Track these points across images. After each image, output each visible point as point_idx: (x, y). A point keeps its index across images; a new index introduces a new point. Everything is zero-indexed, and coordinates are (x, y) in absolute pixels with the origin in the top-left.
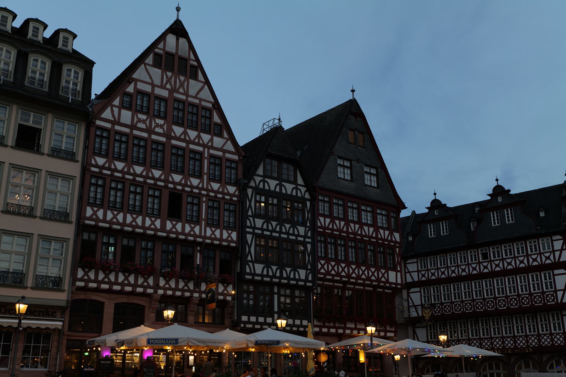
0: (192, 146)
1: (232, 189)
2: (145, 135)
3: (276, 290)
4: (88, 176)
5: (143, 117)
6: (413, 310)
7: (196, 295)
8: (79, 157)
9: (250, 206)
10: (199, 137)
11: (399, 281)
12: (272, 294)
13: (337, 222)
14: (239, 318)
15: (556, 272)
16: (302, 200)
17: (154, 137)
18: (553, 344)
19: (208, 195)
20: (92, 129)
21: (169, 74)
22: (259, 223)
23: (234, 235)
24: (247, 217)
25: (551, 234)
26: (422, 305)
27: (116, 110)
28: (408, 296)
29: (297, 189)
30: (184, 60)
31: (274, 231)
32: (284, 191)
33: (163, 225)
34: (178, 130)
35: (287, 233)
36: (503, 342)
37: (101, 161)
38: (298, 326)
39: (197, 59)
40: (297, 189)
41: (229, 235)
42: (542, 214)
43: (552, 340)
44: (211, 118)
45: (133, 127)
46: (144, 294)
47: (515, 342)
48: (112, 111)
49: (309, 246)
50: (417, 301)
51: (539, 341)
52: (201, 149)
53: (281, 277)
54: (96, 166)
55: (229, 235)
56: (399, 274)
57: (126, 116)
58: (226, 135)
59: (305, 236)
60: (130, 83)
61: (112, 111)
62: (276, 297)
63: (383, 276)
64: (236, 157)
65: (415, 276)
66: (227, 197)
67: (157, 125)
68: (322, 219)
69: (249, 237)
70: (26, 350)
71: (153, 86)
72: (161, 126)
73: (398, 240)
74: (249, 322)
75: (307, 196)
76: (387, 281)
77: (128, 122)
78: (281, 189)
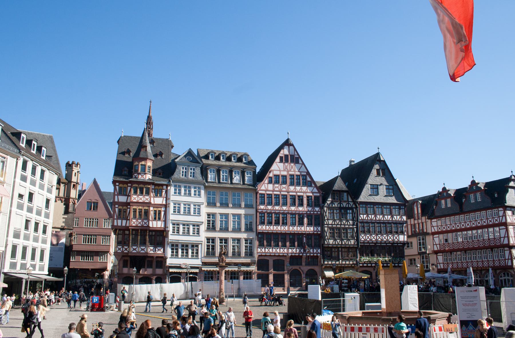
0: (298, 194)
1: (317, 209)
2: (278, 193)
3: (340, 249)
4: (258, 214)
5: (277, 185)
6: (435, 246)
7: (305, 254)
8: (255, 206)
9: (326, 215)
10: (301, 189)
11: (406, 240)
12: (338, 251)
13: (370, 216)
14: (324, 262)
15: (501, 227)
16: (351, 208)
17: (282, 193)
18: (500, 265)
19: (307, 213)
20: (258, 195)
21: (286, 164)
22: (330, 222)
23: (319, 229)
24: (325, 220)
25: (498, 208)
26: (439, 244)
27: (266, 185)
28: (433, 239)
29: (348, 204)
30: (292, 156)
31: (338, 224)
32: (342, 206)
33: (289, 228)
34: (292, 188)
35: (345, 225)
36: (477, 264)
37: (262, 207)
38: (352, 265)
39: (298, 154)
40: (348, 204)
41: (317, 229)
42: (496, 195)
43: (500, 263)
44: (306, 179)
45: (273, 191)
46: (283, 256)
47: (483, 264)
48: (265, 186)
49: (355, 229)
50: (437, 243)
51: (494, 263)
52: (302, 194)
53: (342, 244)
54: (261, 209)
55: (317, 229)
56: (406, 237)
57: (270, 187)
58: (313, 185)
59: (353, 225)
60: (270, 172)
61: (265, 186)
62: (340, 253)
63: (396, 238)
64: (318, 194)
65: (436, 228)
66: (316, 213)
67: (283, 188)
68: (362, 216)
69: (326, 229)
70: (244, 279)
71: (280, 171)
72: (285, 188)
73: (405, 220)
74: (328, 264)
75: (354, 206)
76: (399, 240)
77: (272, 189)
78: (340, 205)
